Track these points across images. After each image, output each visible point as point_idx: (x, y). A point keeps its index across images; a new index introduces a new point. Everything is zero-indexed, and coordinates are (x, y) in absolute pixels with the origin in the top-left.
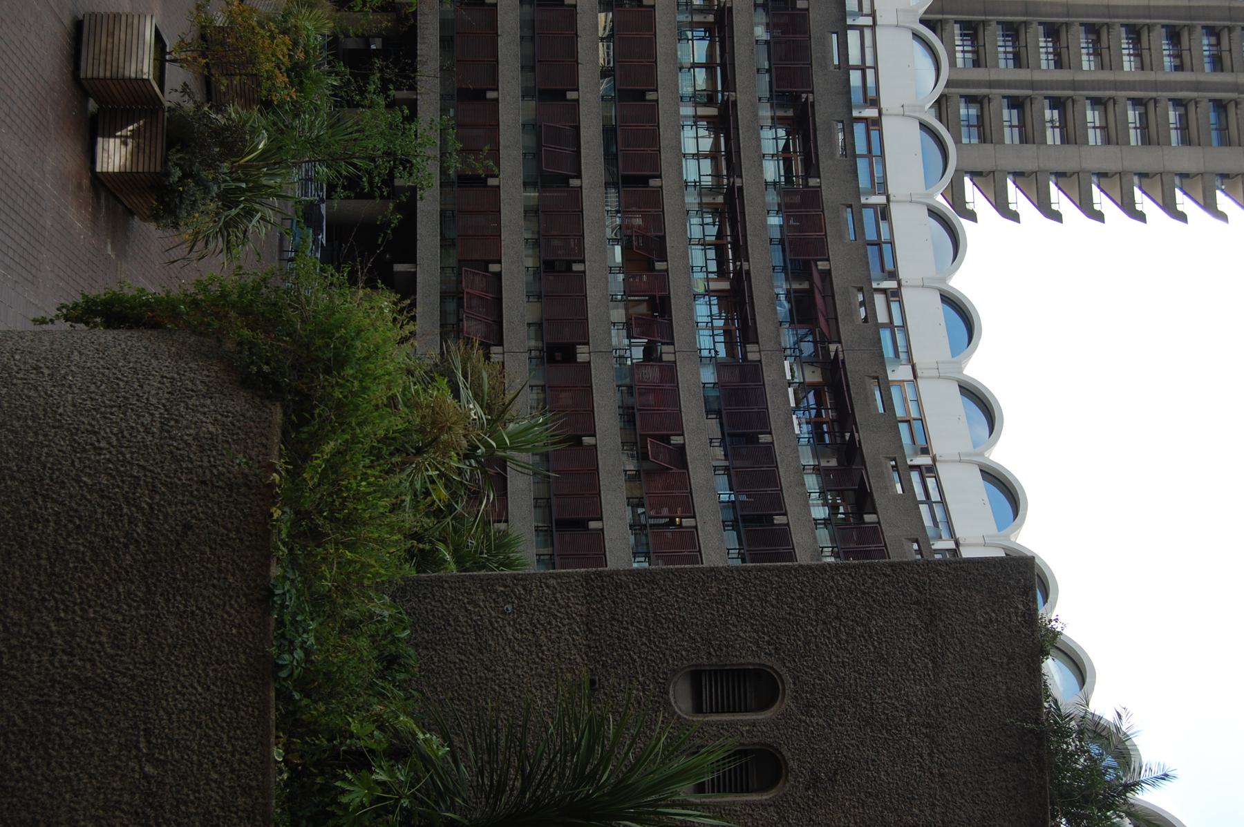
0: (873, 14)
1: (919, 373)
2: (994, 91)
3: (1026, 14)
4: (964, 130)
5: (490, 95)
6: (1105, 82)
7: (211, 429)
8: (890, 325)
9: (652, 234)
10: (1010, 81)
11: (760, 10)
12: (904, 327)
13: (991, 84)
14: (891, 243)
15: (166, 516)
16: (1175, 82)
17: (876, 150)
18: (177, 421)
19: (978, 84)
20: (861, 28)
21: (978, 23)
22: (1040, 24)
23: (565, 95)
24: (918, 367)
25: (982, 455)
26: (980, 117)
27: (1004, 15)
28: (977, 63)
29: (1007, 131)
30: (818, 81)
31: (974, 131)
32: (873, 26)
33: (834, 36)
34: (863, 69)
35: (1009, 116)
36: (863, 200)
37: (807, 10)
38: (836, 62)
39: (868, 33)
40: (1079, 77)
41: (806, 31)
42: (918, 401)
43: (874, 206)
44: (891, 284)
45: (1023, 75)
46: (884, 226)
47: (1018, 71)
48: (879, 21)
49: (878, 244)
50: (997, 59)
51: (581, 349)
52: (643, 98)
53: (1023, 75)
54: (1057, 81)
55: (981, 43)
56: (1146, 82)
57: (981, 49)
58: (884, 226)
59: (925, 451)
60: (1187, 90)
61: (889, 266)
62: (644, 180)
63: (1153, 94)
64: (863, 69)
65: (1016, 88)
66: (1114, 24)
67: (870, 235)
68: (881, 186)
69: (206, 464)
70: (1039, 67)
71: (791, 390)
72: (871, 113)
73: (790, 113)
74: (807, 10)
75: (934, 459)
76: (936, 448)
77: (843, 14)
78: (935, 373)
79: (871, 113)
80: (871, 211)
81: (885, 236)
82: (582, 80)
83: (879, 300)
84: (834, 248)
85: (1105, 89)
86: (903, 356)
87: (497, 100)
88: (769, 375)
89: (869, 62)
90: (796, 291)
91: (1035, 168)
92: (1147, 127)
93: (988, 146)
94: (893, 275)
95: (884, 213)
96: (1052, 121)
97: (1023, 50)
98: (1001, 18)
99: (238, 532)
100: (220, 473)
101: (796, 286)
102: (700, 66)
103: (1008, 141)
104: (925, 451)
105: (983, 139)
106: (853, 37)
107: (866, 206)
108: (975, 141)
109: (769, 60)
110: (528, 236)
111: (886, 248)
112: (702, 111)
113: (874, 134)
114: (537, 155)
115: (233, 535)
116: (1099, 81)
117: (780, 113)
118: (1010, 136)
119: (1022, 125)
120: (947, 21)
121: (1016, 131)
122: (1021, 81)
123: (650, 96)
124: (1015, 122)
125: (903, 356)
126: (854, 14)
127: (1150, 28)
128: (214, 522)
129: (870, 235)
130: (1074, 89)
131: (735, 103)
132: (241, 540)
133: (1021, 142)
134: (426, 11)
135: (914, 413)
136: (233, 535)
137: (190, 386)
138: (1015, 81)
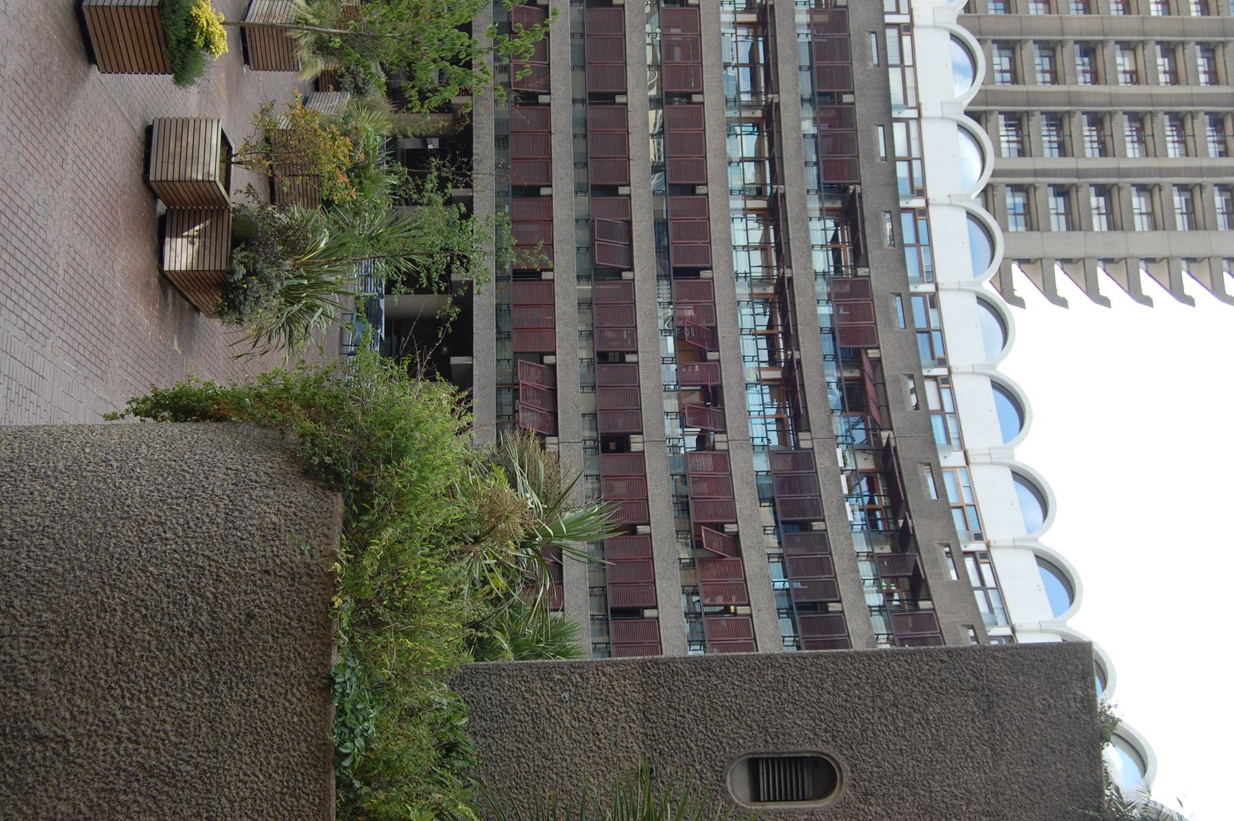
0: (918, 107)
1: (971, 459)
2: (1039, 180)
3: (1070, 104)
4: (1011, 219)
5: (622, 190)
6: (1150, 169)
7: (274, 519)
8: (941, 412)
9: (704, 324)
10: (1055, 170)
11: (807, 105)
12: (955, 413)
13: (1036, 173)
14: (941, 330)
15: (229, 606)
16: (1221, 168)
17: (923, 239)
18: (241, 512)
19: (1023, 173)
20: (906, 121)
21: (1023, 113)
22: (1084, 113)
24: (970, 454)
25: (1036, 540)
26: (1027, 206)
27: (1048, 105)
28: (1022, 153)
29: (1053, 219)
30: (866, 173)
31: (1021, 219)
32: (919, 119)
33: (881, 129)
34: (909, 161)
35: (1056, 204)
36: (912, 289)
37: (853, 104)
38: (883, 154)
39: (913, 125)
40: (1124, 164)
41: (853, 125)
42: (971, 487)
43: (922, 295)
44: (941, 371)
45: (1068, 163)
46: (933, 313)
47: (1063, 159)
48: (924, 113)
50: (1041, 149)
51: (634, 438)
52: (693, 192)
53: (1068, 163)
55: (1026, 133)
56: (1191, 168)
57: (1026, 139)
58: (933, 313)
59: (979, 537)
61: (939, 354)
62: (695, 272)
63: (1199, 180)
64: (909, 161)
65: (1061, 176)
66: (1157, 112)
67: (920, 323)
68: (930, 275)
69: (269, 554)
70: (1084, 155)
71: (843, 478)
72: (918, 203)
73: (838, 205)
74: (853, 104)
75: (988, 546)
76: (991, 533)
77: (888, 107)
78: (987, 459)
79: (918, 203)
81: (934, 324)
83: (930, 387)
84: (883, 336)
85: (1151, 176)
86: (955, 442)
87: (551, 196)
88: (821, 462)
89: (915, 153)
90: (847, 379)
91: (1083, 255)
92: (1194, 212)
93: (1035, 234)
94: (943, 362)
95: (933, 301)
96: (1098, 208)
97: (1067, 139)
98: (1044, 108)
99: (300, 621)
100: (283, 563)
101: (846, 374)
102: (749, 160)
103: (1054, 228)
105: (1030, 226)
106: (899, 130)
107: (916, 294)
108: (1022, 228)
109: (817, 153)
110: (582, 328)
112: (752, 204)
113: (922, 224)
114: (590, 249)
115: (295, 624)
116: (1143, 168)
117: (828, 205)
118: (1057, 223)
119: (1068, 213)
120: (991, 112)
121: (1062, 218)
123: (700, 190)
124: (1062, 210)
125: (955, 442)
126: (899, 107)
127: (1193, 115)
128: (277, 611)
129: (920, 323)
130: (1120, 177)
131: (783, 196)
132: (303, 629)
133: (1068, 229)
134: (482, 111)
135: (967, 500)
136: (295, 624)
137: (254, 477)
138: (1060, 170)
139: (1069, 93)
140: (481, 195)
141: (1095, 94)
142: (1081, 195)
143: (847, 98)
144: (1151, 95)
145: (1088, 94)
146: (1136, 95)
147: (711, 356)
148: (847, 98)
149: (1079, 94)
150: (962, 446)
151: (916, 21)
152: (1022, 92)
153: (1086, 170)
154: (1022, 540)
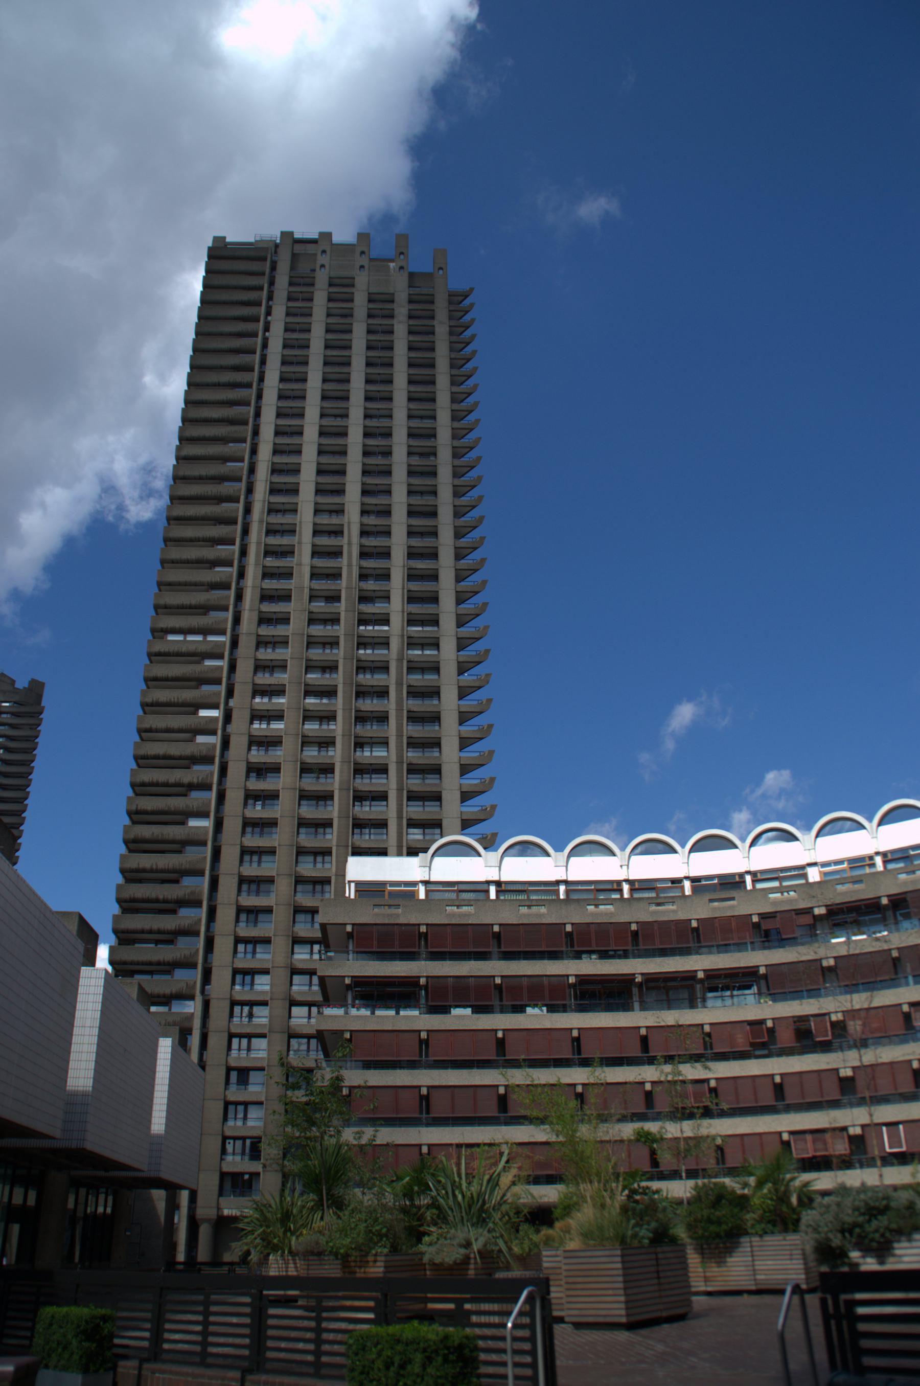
3: (349, 790)
10: (397, 804)
40: (394, 758)
47: (390, 799)
54: (397, 773)
56: (397, 716)
60: (402, 690)
63: (405, 712)
84: (681, 916)
88: (843, 952)
104: (871, 858)
116: (397, 746)
121: (426, 803)
122: (397, 797)
124: (421, 803)
138: (397, 801)
139: (340, 789)
141: (341, 772)
142: (415, 789)
144: (343, 735)
145: (341, 776)
146: (343, 745)
147: (770, 1024)
149: (341, 783)
152: (339, 821)
153: (397, 784)
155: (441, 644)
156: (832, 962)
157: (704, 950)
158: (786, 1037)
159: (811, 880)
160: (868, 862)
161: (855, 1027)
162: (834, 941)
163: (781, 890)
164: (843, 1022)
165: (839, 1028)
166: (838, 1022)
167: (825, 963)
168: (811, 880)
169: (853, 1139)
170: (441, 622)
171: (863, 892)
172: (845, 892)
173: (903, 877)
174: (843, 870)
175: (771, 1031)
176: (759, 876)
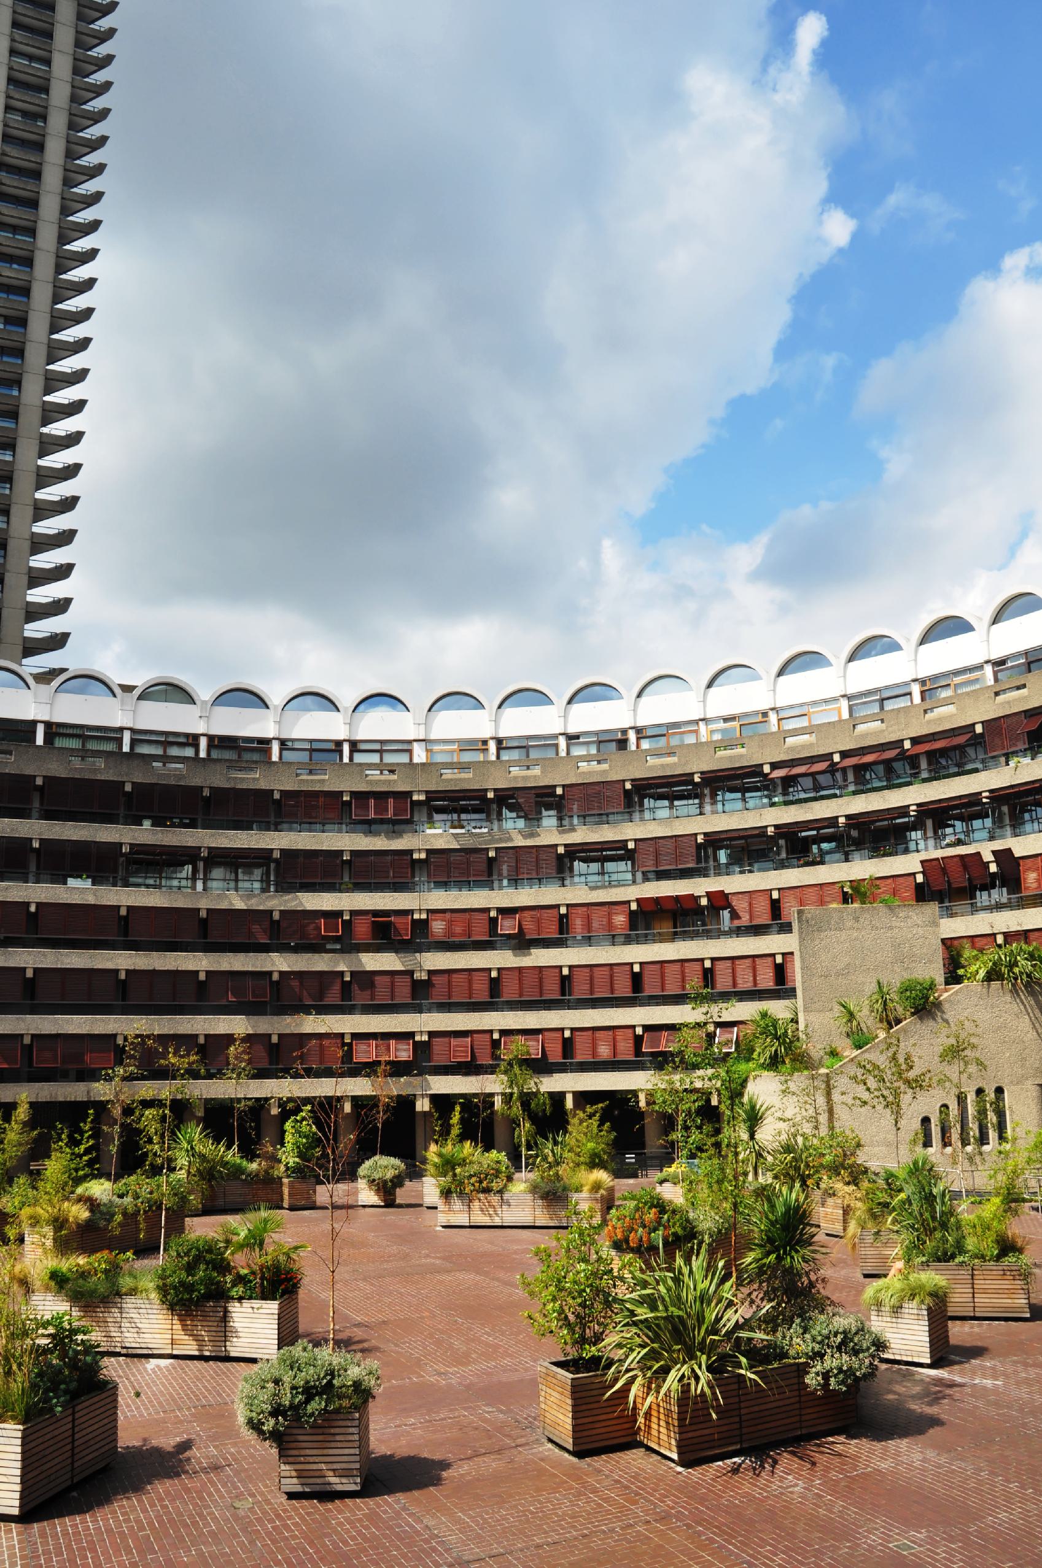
0: (121, 729)
14: (311, 741)
23: (202, 982)
43: (281, 750)
46: (297, 745)
48: (130, 725)
49: (312, 750)
51: (417, 976)
61: (332, 746)
64: (166, 744)
67: (304, 757)
75: (492, 738)
80: (285, 753)
82: (191, 968)
87: (206, 1036)
94: (339, 744)
111: (315, 746)
125: (405, 747)
129: (304, 757)
131: (209, 848)
140: (204, 1092)
143: (128, 788)
148: (128, 788)
150: (410, 742)
151: (46, 718)
154: (490, 715)
155: (24, 383)
156: (423, 856)
157: (285, 826)
158: (362, 929)
159: (416, 760)
160: (480, 746)
161: (438, 927)
162: (429, 831)
163: (380, 767)
164: (426, 921)
165: (421, 927)
166: (420, 920)
167: (416, 856)
168: (416, 760)
169: (417, 1045)
170: (27, 354)
171: (467, 780)
172: (453, 779)
173: (515, 770)
174: (453, 751)
175: (348, 925)
176: (363, 747)
